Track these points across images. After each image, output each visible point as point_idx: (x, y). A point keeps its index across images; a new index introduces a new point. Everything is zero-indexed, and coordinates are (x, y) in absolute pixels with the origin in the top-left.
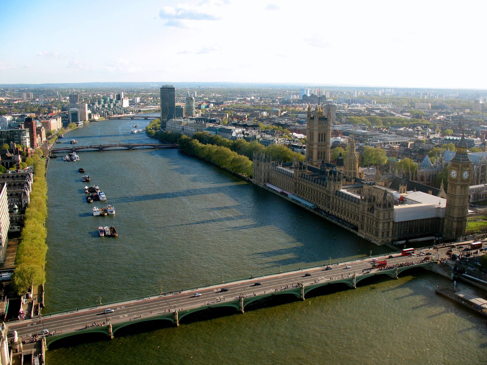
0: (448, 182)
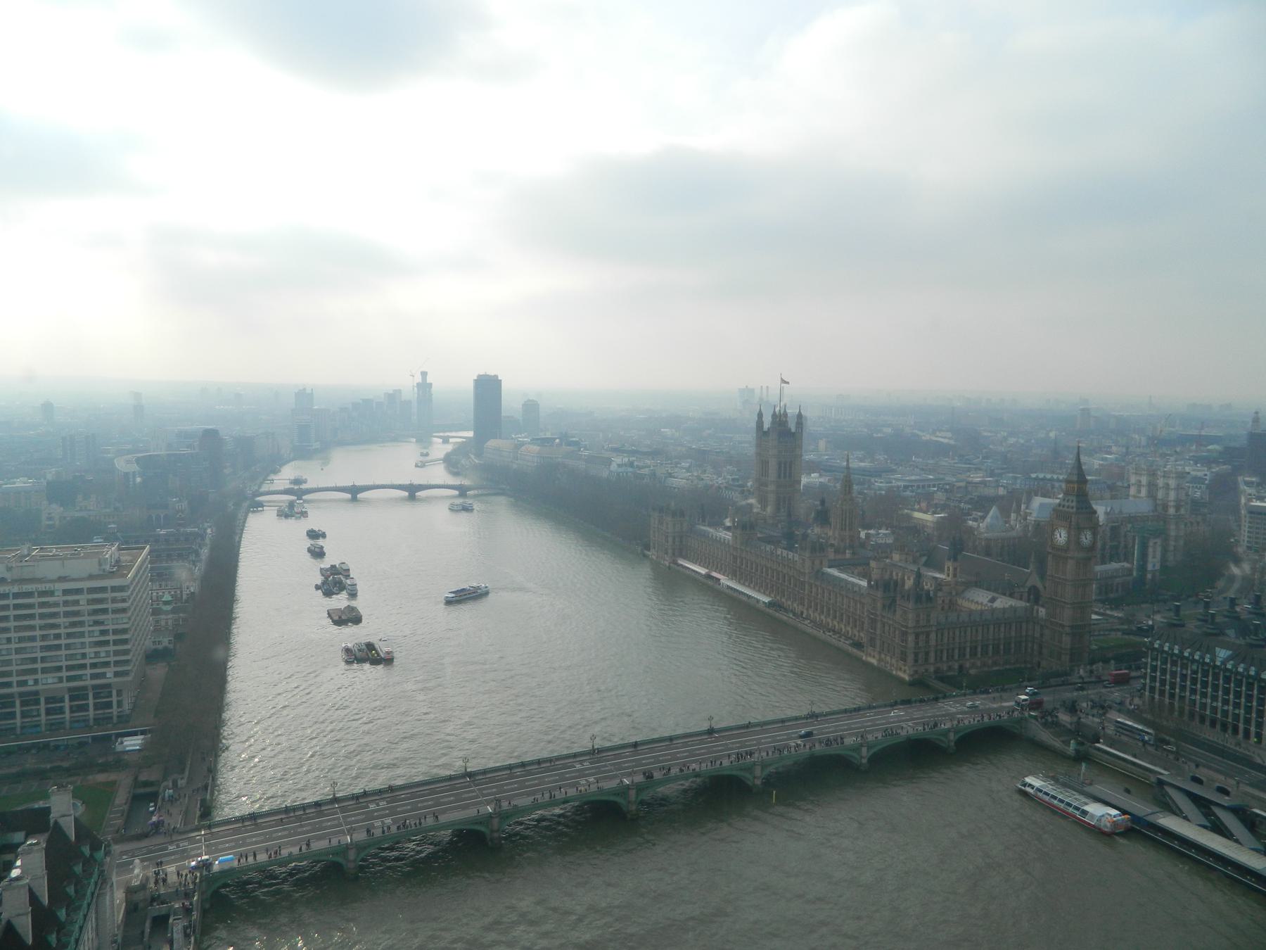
0: (1050, 553)
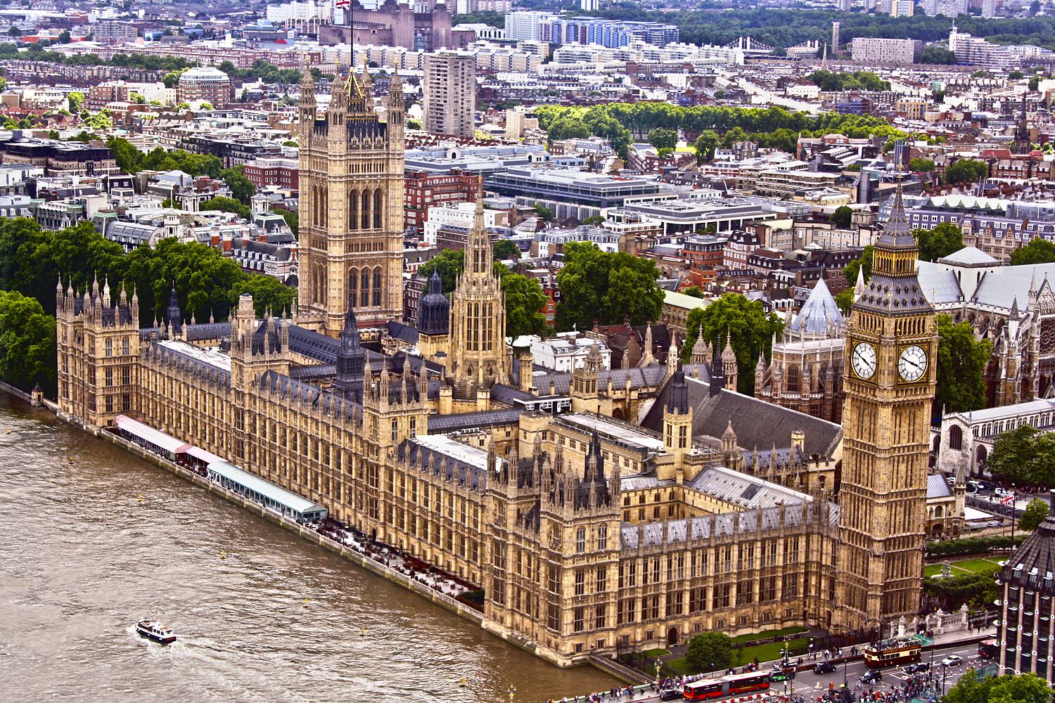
0: (845, 394)
